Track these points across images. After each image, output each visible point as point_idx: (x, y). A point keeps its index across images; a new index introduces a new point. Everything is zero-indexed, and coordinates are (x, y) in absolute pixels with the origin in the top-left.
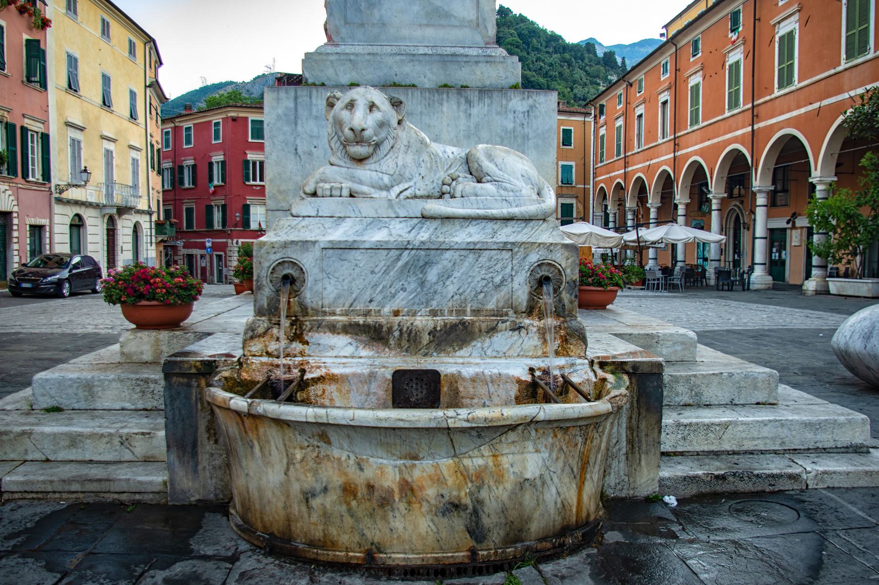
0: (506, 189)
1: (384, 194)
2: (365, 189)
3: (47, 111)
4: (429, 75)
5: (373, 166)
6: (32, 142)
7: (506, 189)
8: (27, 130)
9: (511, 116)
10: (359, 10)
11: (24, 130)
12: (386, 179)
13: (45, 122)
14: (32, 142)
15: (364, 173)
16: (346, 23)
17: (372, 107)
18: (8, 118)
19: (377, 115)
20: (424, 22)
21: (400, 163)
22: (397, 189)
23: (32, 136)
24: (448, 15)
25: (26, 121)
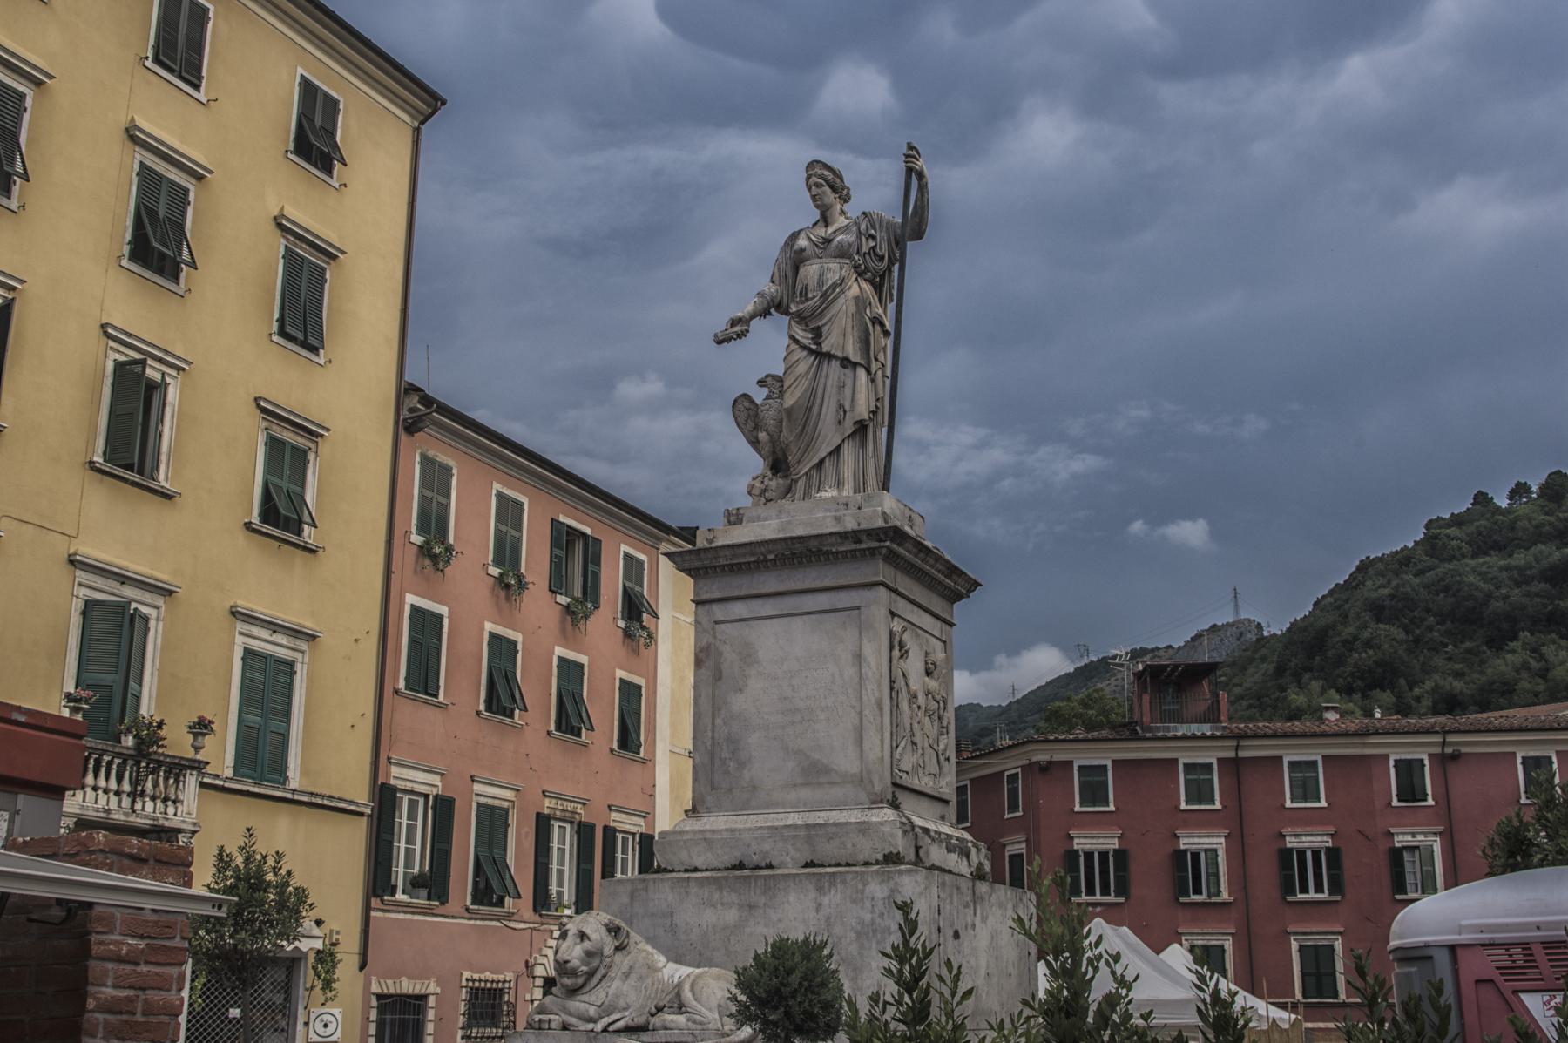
0: (694, 1022)
1: (590, 1026)
2: (573, 1020)
3: (652, 795)
4: (792, 852)
5: (585, 998)
6: (624, 851)
7: (694, 1022)
8: (614, 830)
9: (868, 904)
10: (727, 772)
11: (610, 833)
12: (592, 1011)
13: (648, 815)
14: (624, 851)
15: (576, 1004)
16: (713, 788)
17: (583, 936)
18: (583, 814)
19: (587, 944)
20: (800, 781)
21: (611, 991)
22: (606, 1021)
23: (625, 840)
24: (826, 770)
25: (614, 815)
